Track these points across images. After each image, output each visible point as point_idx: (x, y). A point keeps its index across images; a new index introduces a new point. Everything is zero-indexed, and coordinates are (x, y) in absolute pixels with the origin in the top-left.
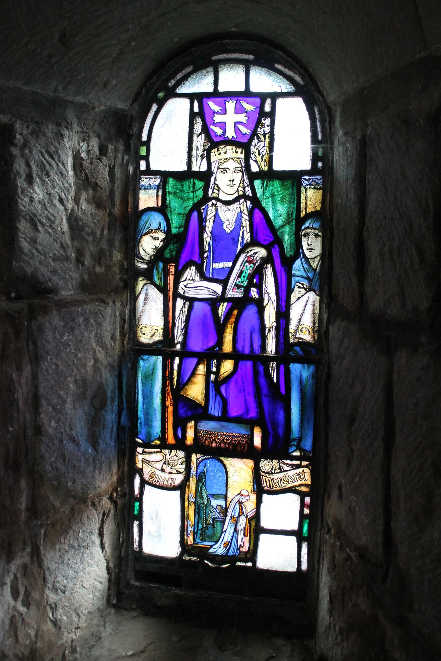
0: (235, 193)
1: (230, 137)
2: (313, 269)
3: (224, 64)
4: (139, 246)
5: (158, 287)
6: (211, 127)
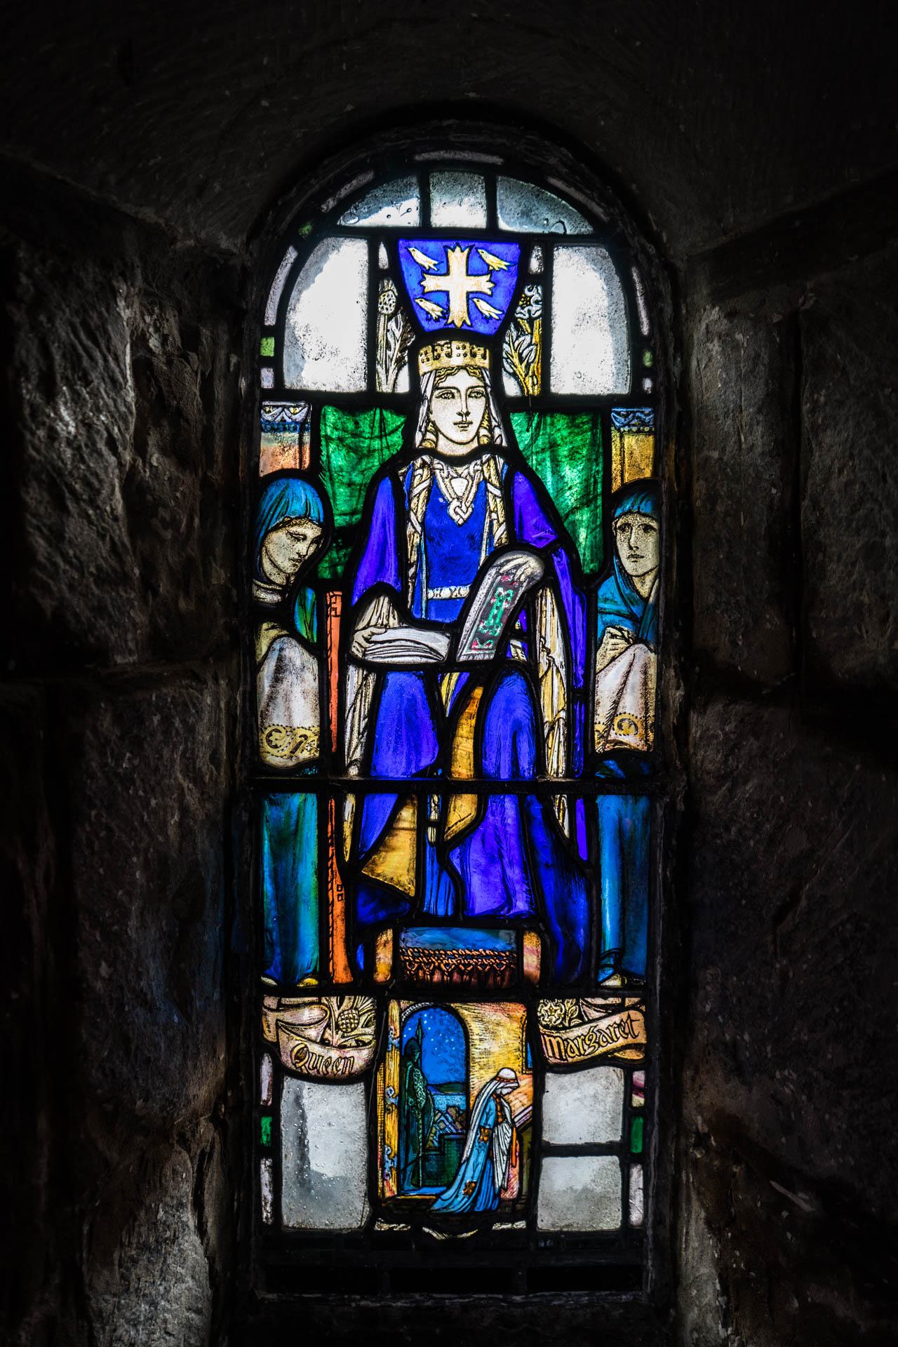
1: (458, 324)
2: (641, 597)
3: (441, 172)
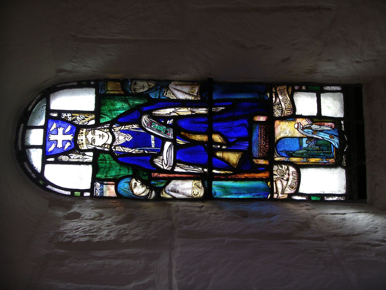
0: (108, 134)
1: (72, 137)
2: (155, 86)
4: (140, 196)
5: (167, 184)
6: (65, 149)
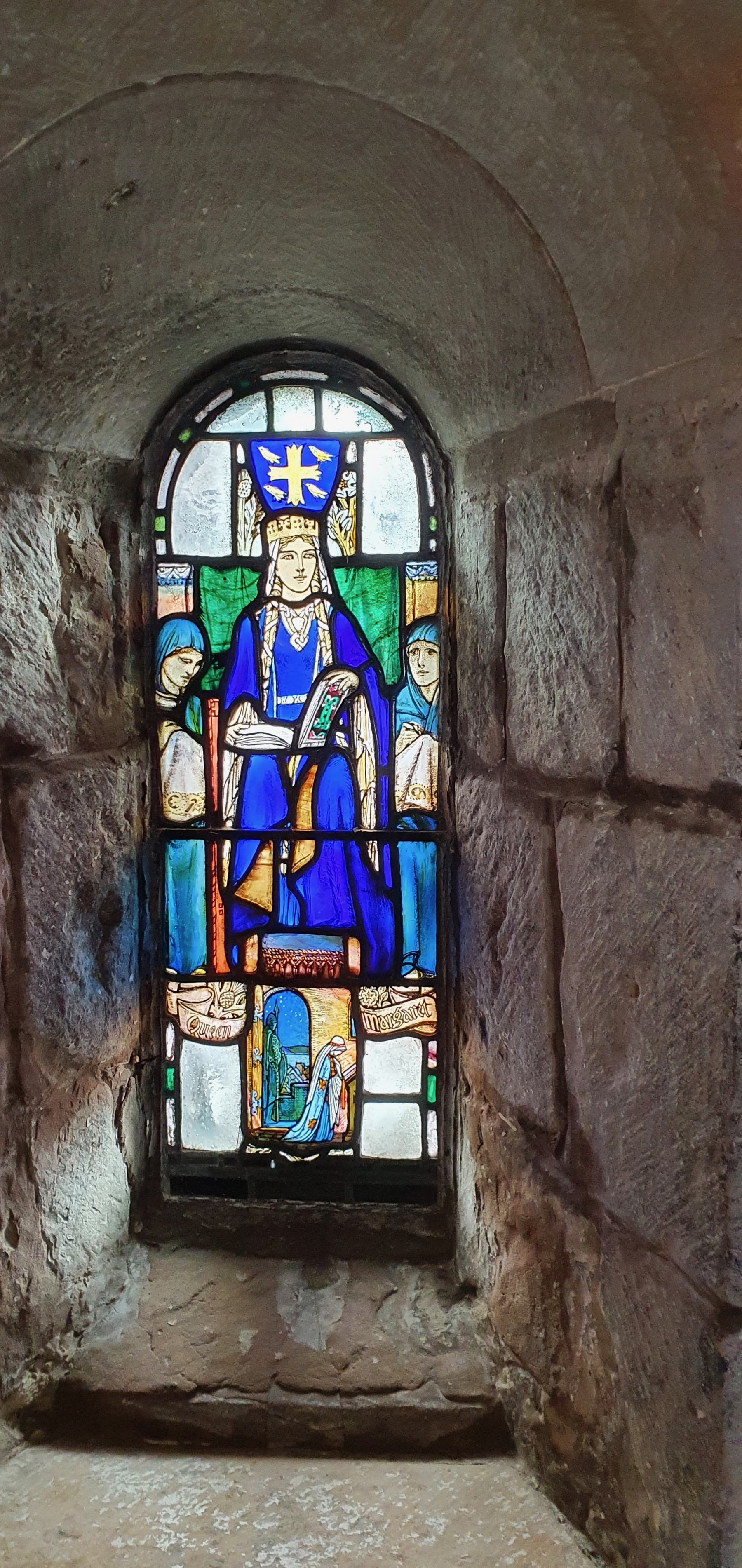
1: (296, 504)
2: (427, 701)
4: (160, 672)
6: (265, 487)
